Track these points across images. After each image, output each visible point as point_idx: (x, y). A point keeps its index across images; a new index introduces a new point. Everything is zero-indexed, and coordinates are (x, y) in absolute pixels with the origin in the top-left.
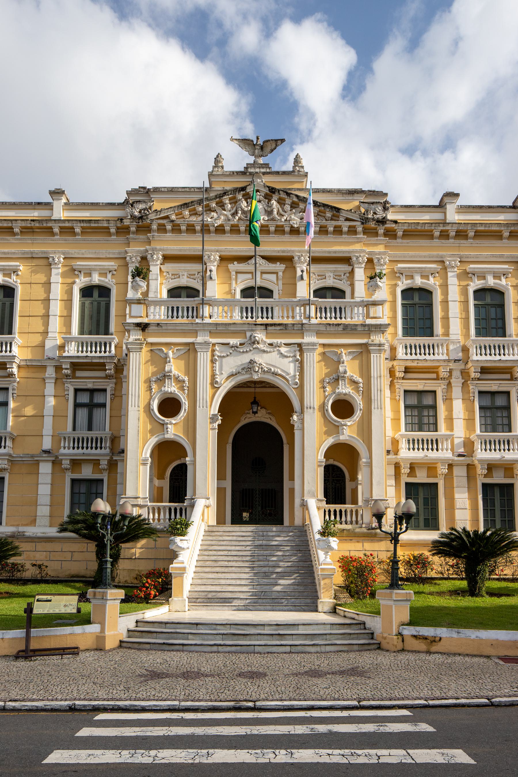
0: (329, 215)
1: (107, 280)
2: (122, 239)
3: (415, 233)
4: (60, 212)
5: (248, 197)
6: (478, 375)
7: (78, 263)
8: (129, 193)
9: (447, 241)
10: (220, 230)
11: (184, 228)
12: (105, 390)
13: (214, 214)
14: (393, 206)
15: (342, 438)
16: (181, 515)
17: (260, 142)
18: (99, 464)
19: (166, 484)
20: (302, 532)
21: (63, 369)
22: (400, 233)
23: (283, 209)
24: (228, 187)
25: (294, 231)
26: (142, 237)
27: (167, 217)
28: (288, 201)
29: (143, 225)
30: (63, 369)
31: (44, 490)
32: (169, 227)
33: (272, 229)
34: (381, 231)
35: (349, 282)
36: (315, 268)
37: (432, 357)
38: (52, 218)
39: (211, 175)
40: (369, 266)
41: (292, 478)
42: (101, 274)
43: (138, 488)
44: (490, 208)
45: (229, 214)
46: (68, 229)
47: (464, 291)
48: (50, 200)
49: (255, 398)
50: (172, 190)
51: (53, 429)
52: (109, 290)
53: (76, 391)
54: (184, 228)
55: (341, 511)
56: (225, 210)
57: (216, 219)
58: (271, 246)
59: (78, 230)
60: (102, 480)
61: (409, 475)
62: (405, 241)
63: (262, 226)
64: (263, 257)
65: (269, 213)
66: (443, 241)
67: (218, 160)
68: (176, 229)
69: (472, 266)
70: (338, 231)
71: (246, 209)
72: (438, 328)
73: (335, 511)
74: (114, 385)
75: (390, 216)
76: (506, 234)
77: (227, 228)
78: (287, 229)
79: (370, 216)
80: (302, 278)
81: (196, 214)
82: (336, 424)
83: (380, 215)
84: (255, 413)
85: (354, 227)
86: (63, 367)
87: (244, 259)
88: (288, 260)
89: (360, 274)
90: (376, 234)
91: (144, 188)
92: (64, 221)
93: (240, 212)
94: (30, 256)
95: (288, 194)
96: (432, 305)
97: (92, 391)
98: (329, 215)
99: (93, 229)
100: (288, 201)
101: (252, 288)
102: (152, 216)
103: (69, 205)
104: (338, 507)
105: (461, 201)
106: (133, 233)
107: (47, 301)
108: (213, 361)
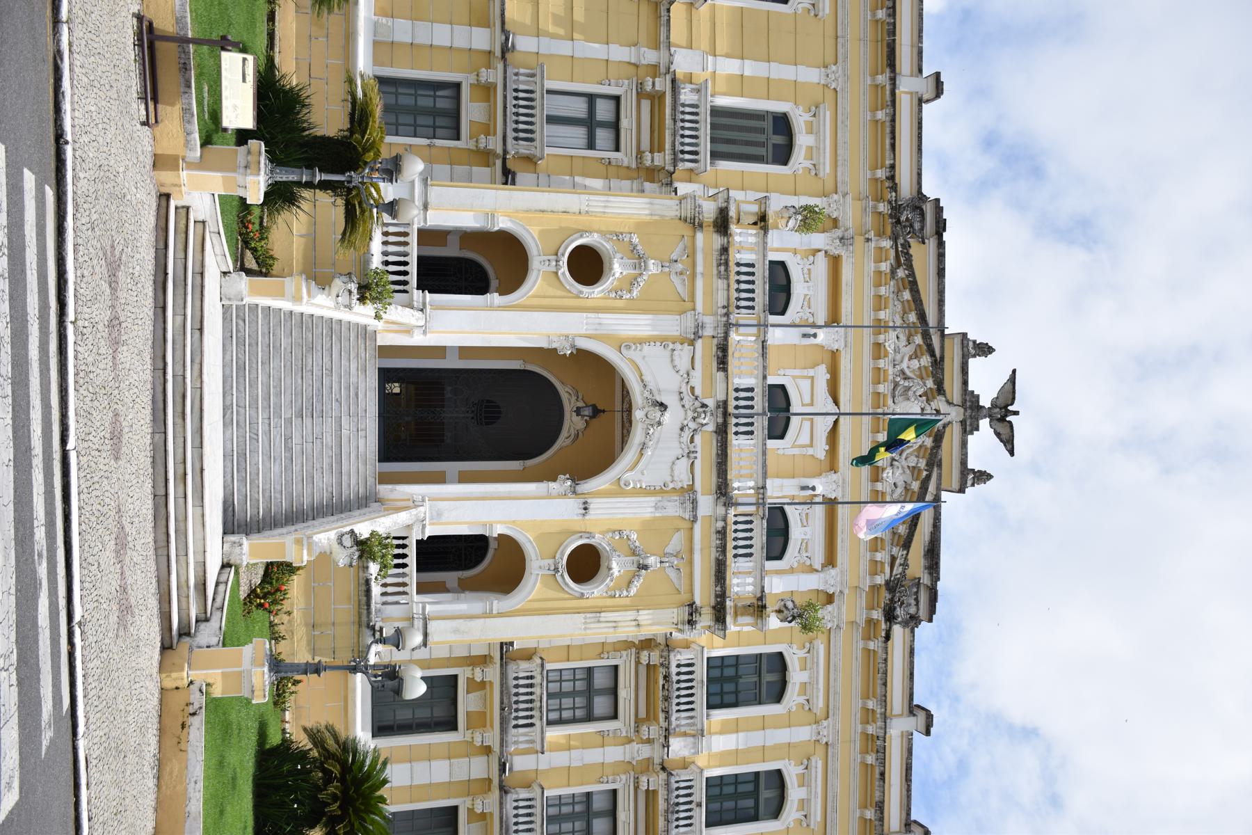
1: (801, 159)
6: (643, 787)
7: (828, 113)
8: (937, 200)
9: (858, 722)
12: (617, 149)
14: (913, 631)
16: (394, 283)
18: (487, 134)
19: (451, 250)
20: (365, 502)
21: (654, 77)
23: (911, 454)
26: (869, 220)
30: (654, 77)
31: (441, 35)
35: (795, 565)
40: (823, 598)
41: (464, 478)
42: (810, 149)
43: (441, 198)
45: (904, 365)
48: (926, 73)
49: (604, 411)
51: (551, 55)
52: (785, 163)
53: (617, 99)
55: (404, 566)
56: (910, 358)
60: (458, 139)
61: (470, 681)
62: (859, 652)
64: (836, 422)
66: (859, 715)
69: (820, 764)
71: (910, 393)
73: (404, 556)
74: (626, 164)
75: (897, 630)
80: (804, 488)
81: (905, 313)
82: (558, 556)
84: (578, 411)
85: (883, 571)
86: (657, 80)
89: (809, 583)
91: (944, 230)
93: (906, 384)
94: (839, 34)
96: (760, 703)
97: (615, 126)
104: (412, 560)
105: (918, 738)
106: (875, 207)
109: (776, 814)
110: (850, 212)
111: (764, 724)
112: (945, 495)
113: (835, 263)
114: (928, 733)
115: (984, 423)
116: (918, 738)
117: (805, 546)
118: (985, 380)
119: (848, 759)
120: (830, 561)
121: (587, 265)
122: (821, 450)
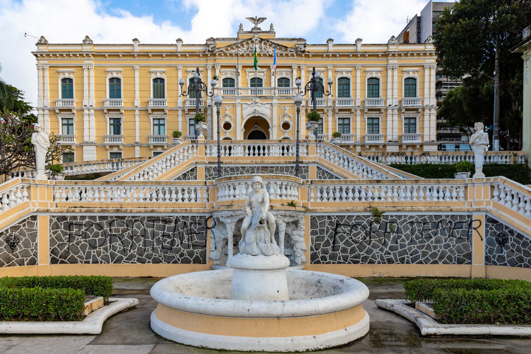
0: (283, 49)
2: (205, 58)
3: (317, 55)
8: (207, 40)
10: (242, 55)
11: (228, 55)
13: (240, 49)
15: (286, 136)
17: (257, 18)
22: (311, 56)
24: (245, 38)
25: (270, 56)
26: (212, 58)
27: (222, 51)
28: (268, 44)
32: (223, 55)
33: (262, 55)
34: (303, 55)
36: (278, 70)
37: (321, 105)
38: (178, 51)
39: (238, 33)
45: (245, 49)
50: (223, 39)
54: (228, 55)
57: (241, 51)
58: (261, 61)
59: (188, 56)
63: (258, 54)
65: (261, 49)
67: (241, 26)
68: (226, 55)
70: (287, 55)
75: (307, 49)
76: (351, 56)
77: (245, 55)
78: (268, 55)
79: (299, 50)
83: (303, 49)
90: (302, 56)
92: (182, 52)
95: (268, 41)
98: (283, 49)
99: (193, 54)
100: (268, 44)
101: (254, 78)
102: (216, 51)
108: (242, 110)
109: (349, 79)
110: (210, 63)
112: (276, 37)
113: (221, 67)
114: (333, 40)
115: (259, 26)
116: (334, 43)
118: (249, 26)
119: (337, 62)
120: (290, 67)
121: (227, 126)
122: (265, 70)
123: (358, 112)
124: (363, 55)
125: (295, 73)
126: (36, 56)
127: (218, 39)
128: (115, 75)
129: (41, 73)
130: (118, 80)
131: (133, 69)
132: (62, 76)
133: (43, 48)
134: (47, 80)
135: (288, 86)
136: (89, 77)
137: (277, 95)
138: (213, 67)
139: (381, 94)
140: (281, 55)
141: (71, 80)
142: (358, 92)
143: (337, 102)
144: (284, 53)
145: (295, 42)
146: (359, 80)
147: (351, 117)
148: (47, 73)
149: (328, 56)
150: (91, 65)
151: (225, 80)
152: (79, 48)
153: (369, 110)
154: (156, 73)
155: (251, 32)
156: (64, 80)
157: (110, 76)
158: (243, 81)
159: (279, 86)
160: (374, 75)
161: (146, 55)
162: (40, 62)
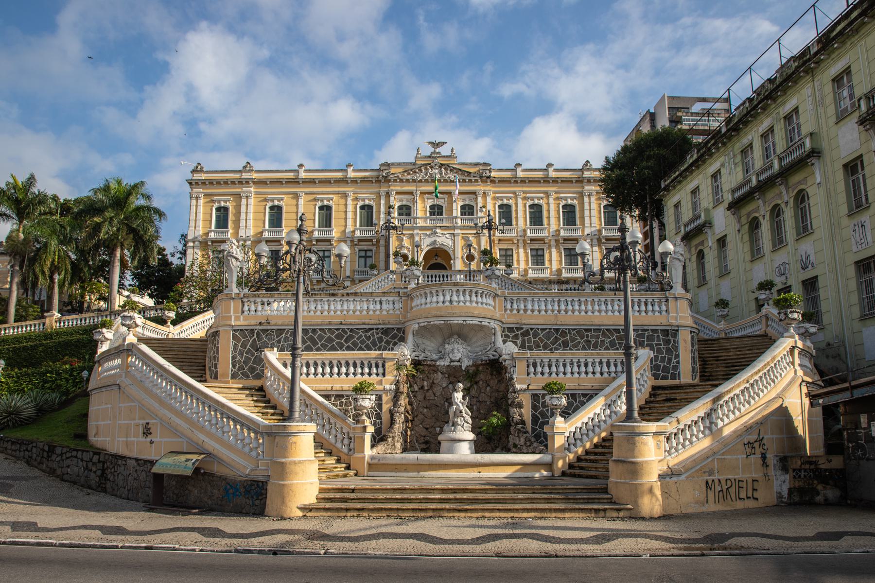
2: (377, 185)
4: (351, 174)
5: (432, 167)
10: (420, 181)
25: (452, 182)
26: (386, 184)
29: (387, 179)
44: (535, 170)
46: (354, 181)
47: (525, 206)
50: (399, 164)
65: (441, 174)
68: (401, 181)
70: (470, 181)
72: (514, 222)
75: (493, 174)
83: (488, 174)
87: (430, 193)
88: (449, 194)
99: (364, 180)
103: (354, 171)
107: (346, 212)
110: (383, 190)
111: (517, 211)
117: (470, 200)
122: (446, 196)
123: (553, 242)
124: (555, 181)
125: (480, 199)
126: (190, 184)
127: (393, 164)
128: (276, 203)
129: (194, 202)
130: (279, 208)
131: (296, 196)
132: (216, 205)
133: (197, 176)
134: (201, 209)
135: (473, 214)
136: (247, 205)
137: (460, 224)
138: (387, 193)
139: (578, 222)
140: (464, 181)
141: (226, 209)
142: (553, 221)
143: (528, 231)
144: (467, 179)
145: (481, 167)
146: (552, 206)
147: (545, 247)
148: (202, 201)
149: (516, 182)
150: (251, 192)
151: (400, 208)
152: (237, 176)
153: (565, 240)
154: (322, 201)
155: (430, 157)
156: (218, 209)
157: (270, 204)
158: (421, 209)
159: (462, 214)
160: (569, 202)
161: (312, 182)
162: (195, 190)
